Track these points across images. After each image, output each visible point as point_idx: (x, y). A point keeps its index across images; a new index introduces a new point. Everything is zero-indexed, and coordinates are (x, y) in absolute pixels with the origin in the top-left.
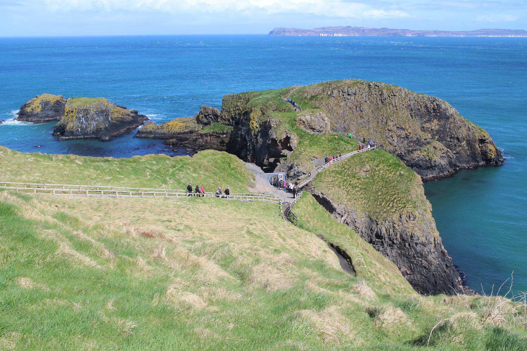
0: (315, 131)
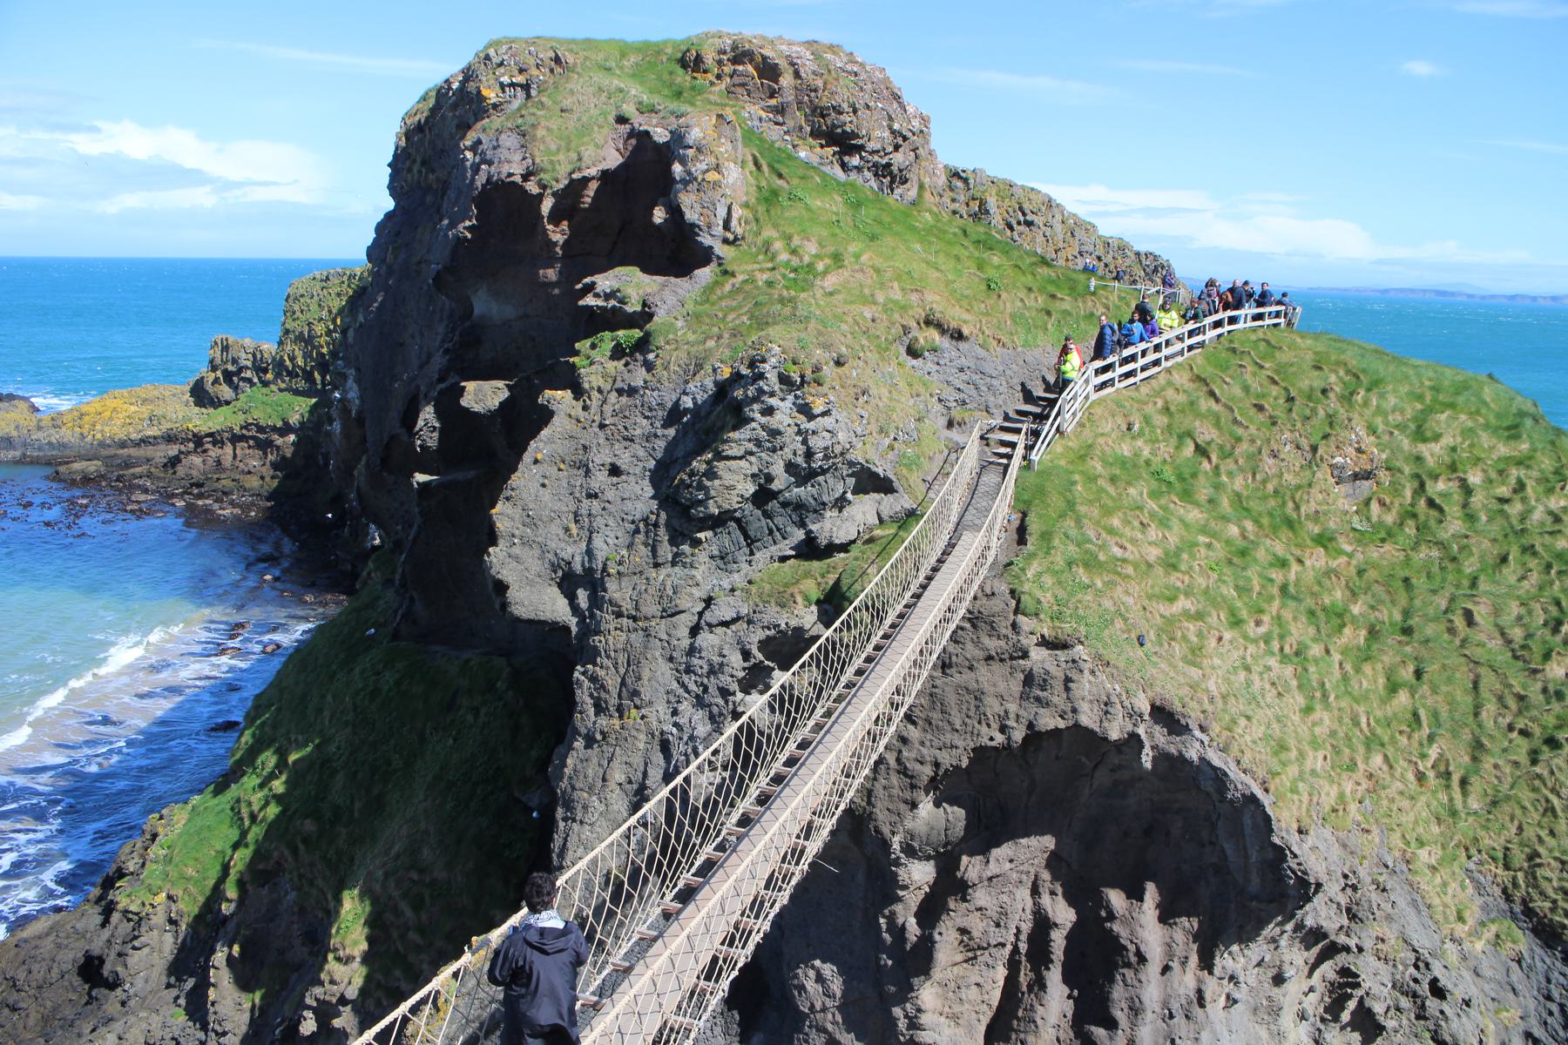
0: (855, 161)
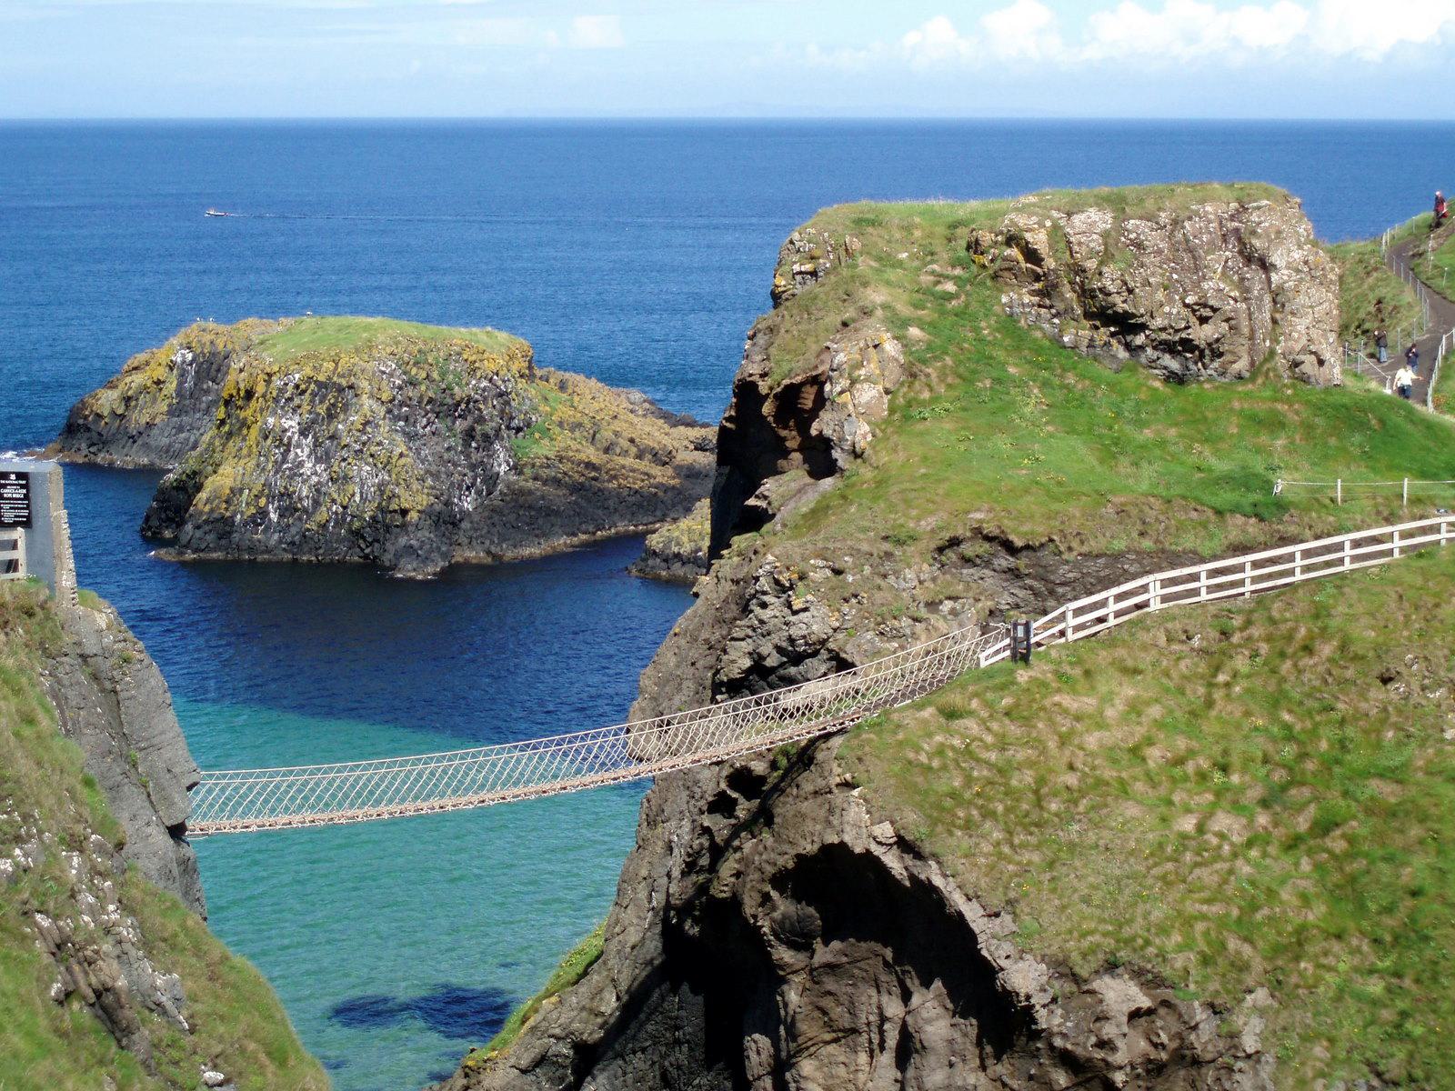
0: (1140, 339)
